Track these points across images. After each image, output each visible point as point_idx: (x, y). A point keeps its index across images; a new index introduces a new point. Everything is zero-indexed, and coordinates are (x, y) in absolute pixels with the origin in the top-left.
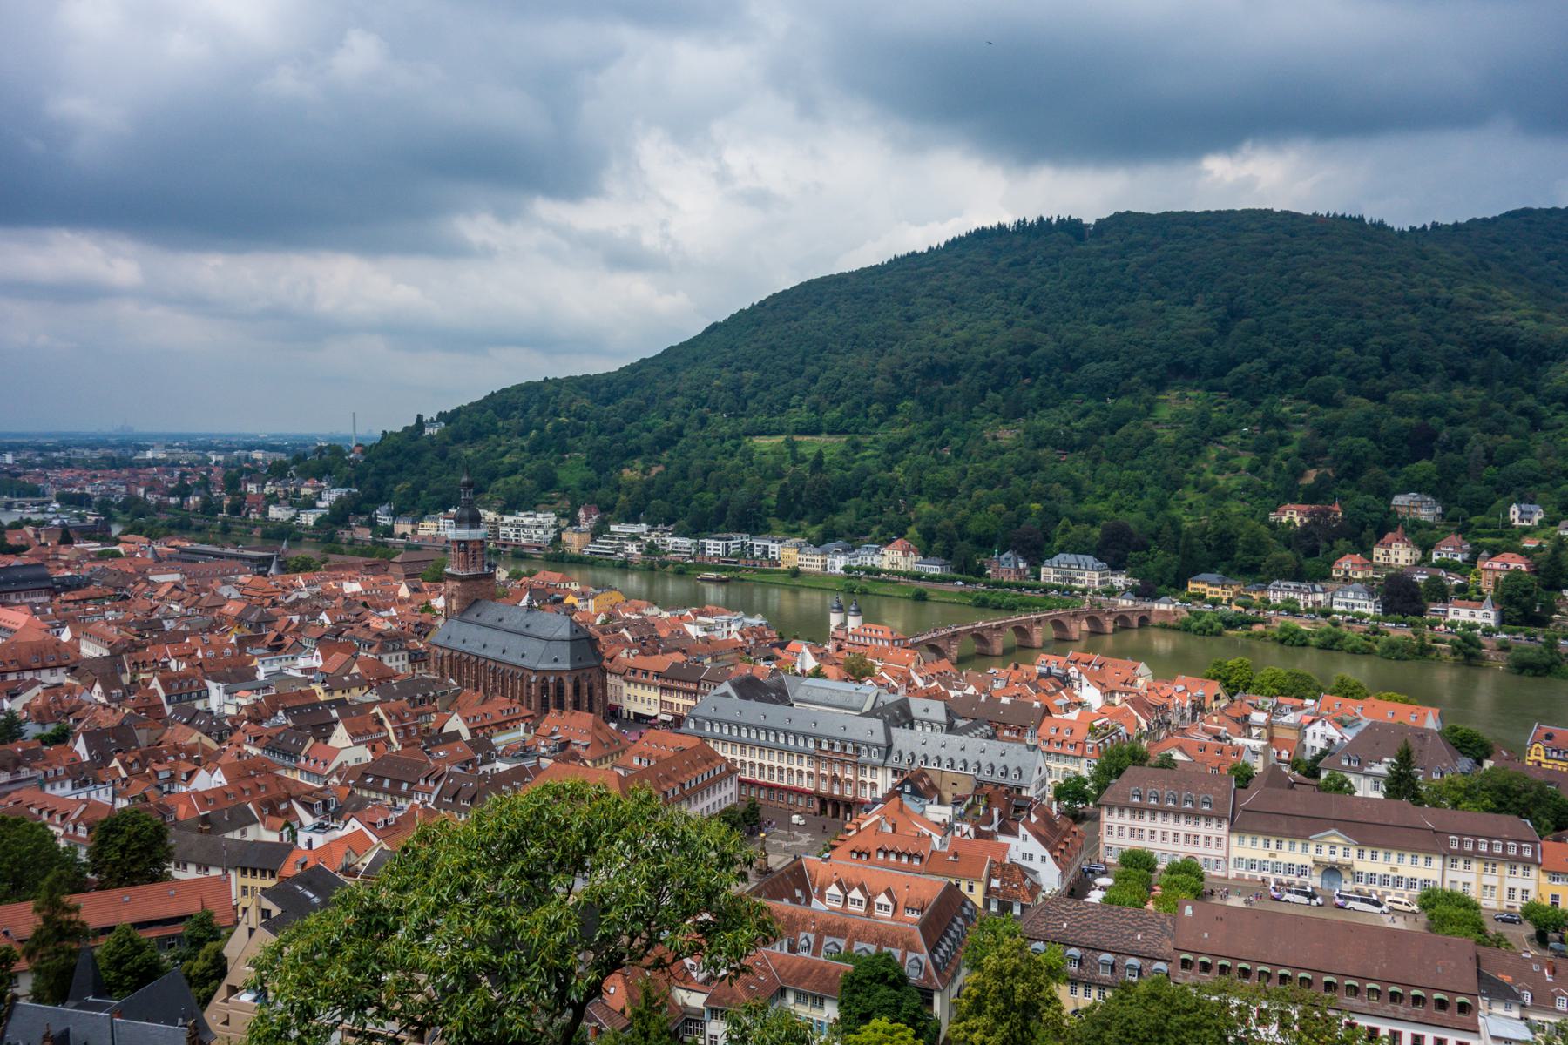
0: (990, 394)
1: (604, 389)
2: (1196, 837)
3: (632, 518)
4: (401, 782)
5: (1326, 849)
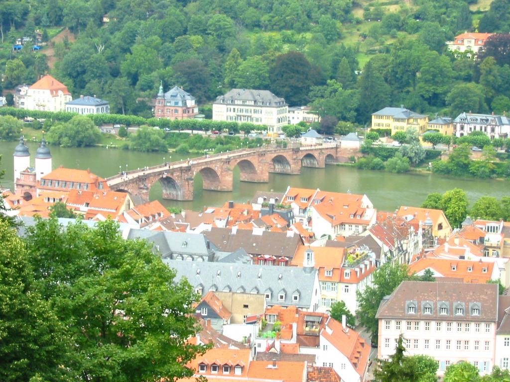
2: (467, 342)
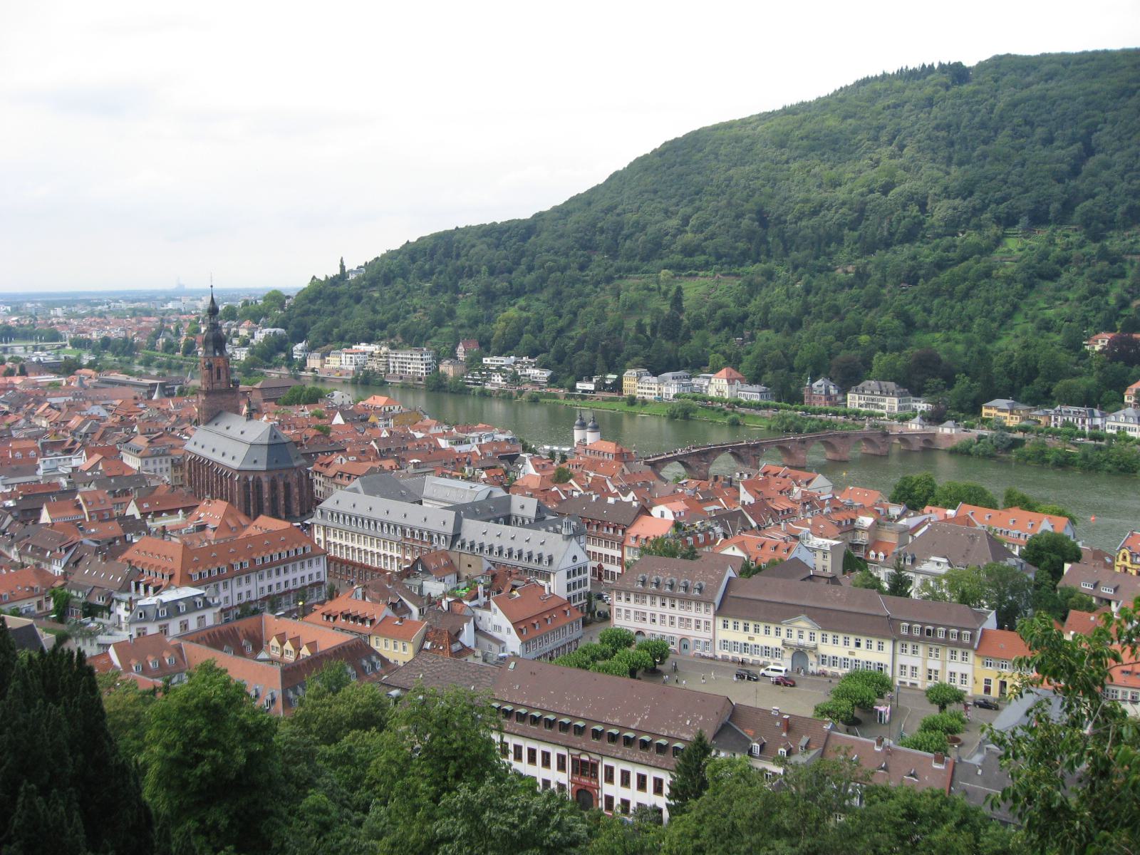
4: (46, 551)
5: (795, 633)
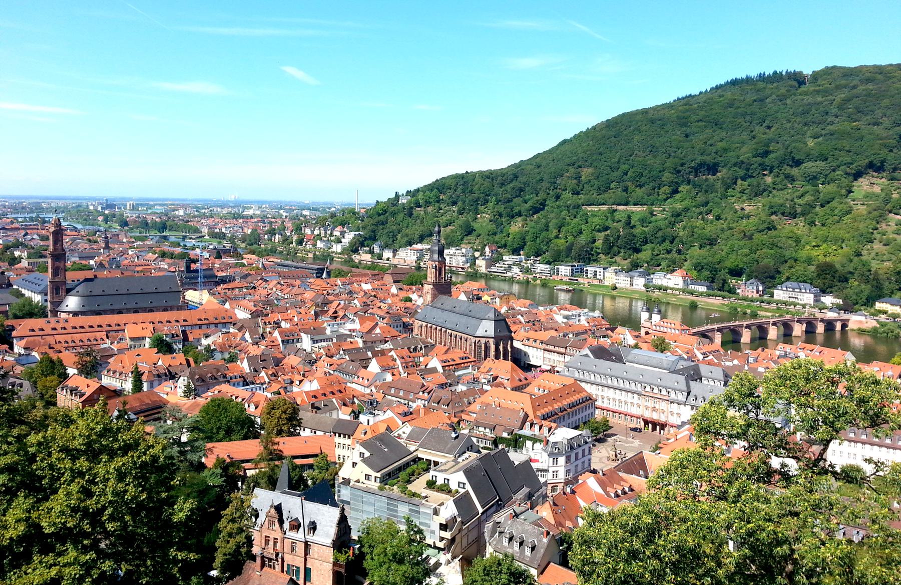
0: (739, 182)
1: (499, 178)
3: (515, 252)
